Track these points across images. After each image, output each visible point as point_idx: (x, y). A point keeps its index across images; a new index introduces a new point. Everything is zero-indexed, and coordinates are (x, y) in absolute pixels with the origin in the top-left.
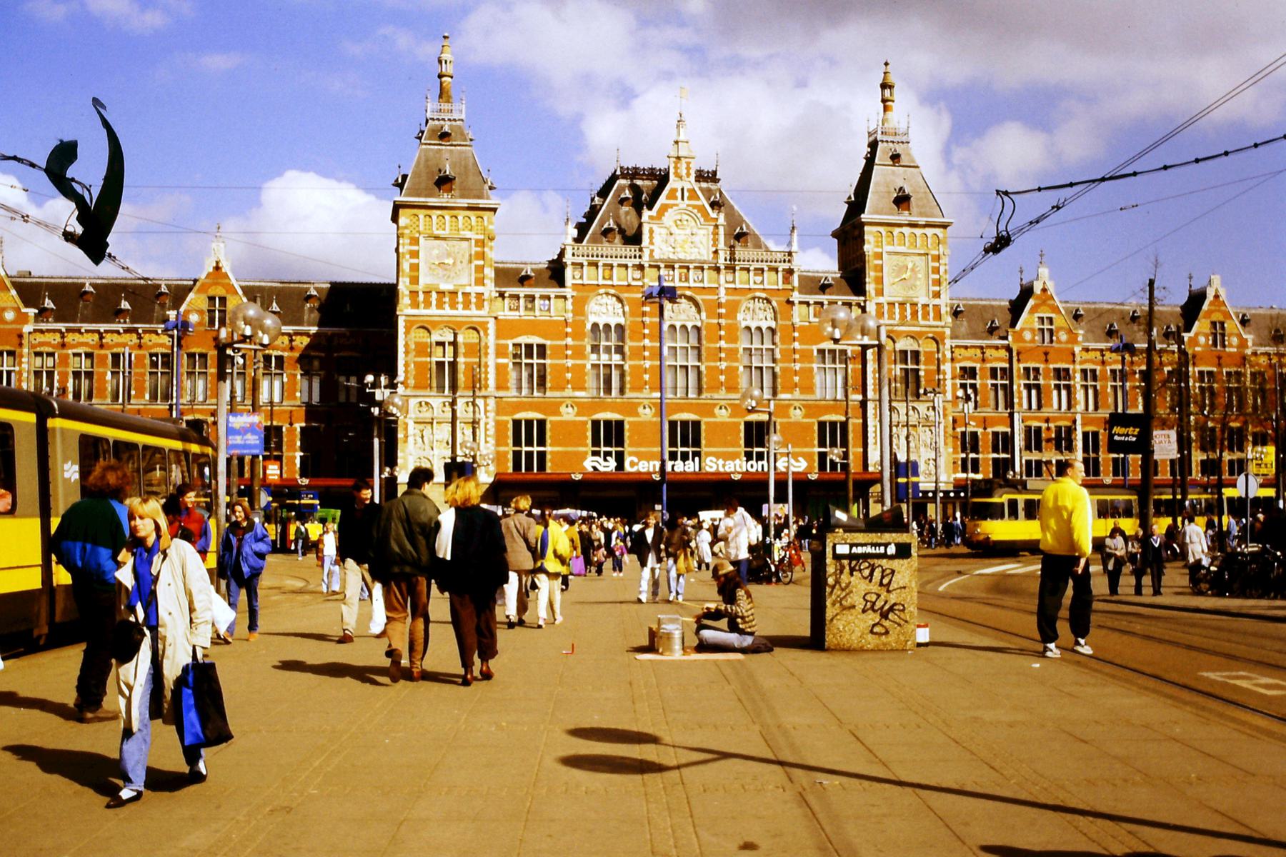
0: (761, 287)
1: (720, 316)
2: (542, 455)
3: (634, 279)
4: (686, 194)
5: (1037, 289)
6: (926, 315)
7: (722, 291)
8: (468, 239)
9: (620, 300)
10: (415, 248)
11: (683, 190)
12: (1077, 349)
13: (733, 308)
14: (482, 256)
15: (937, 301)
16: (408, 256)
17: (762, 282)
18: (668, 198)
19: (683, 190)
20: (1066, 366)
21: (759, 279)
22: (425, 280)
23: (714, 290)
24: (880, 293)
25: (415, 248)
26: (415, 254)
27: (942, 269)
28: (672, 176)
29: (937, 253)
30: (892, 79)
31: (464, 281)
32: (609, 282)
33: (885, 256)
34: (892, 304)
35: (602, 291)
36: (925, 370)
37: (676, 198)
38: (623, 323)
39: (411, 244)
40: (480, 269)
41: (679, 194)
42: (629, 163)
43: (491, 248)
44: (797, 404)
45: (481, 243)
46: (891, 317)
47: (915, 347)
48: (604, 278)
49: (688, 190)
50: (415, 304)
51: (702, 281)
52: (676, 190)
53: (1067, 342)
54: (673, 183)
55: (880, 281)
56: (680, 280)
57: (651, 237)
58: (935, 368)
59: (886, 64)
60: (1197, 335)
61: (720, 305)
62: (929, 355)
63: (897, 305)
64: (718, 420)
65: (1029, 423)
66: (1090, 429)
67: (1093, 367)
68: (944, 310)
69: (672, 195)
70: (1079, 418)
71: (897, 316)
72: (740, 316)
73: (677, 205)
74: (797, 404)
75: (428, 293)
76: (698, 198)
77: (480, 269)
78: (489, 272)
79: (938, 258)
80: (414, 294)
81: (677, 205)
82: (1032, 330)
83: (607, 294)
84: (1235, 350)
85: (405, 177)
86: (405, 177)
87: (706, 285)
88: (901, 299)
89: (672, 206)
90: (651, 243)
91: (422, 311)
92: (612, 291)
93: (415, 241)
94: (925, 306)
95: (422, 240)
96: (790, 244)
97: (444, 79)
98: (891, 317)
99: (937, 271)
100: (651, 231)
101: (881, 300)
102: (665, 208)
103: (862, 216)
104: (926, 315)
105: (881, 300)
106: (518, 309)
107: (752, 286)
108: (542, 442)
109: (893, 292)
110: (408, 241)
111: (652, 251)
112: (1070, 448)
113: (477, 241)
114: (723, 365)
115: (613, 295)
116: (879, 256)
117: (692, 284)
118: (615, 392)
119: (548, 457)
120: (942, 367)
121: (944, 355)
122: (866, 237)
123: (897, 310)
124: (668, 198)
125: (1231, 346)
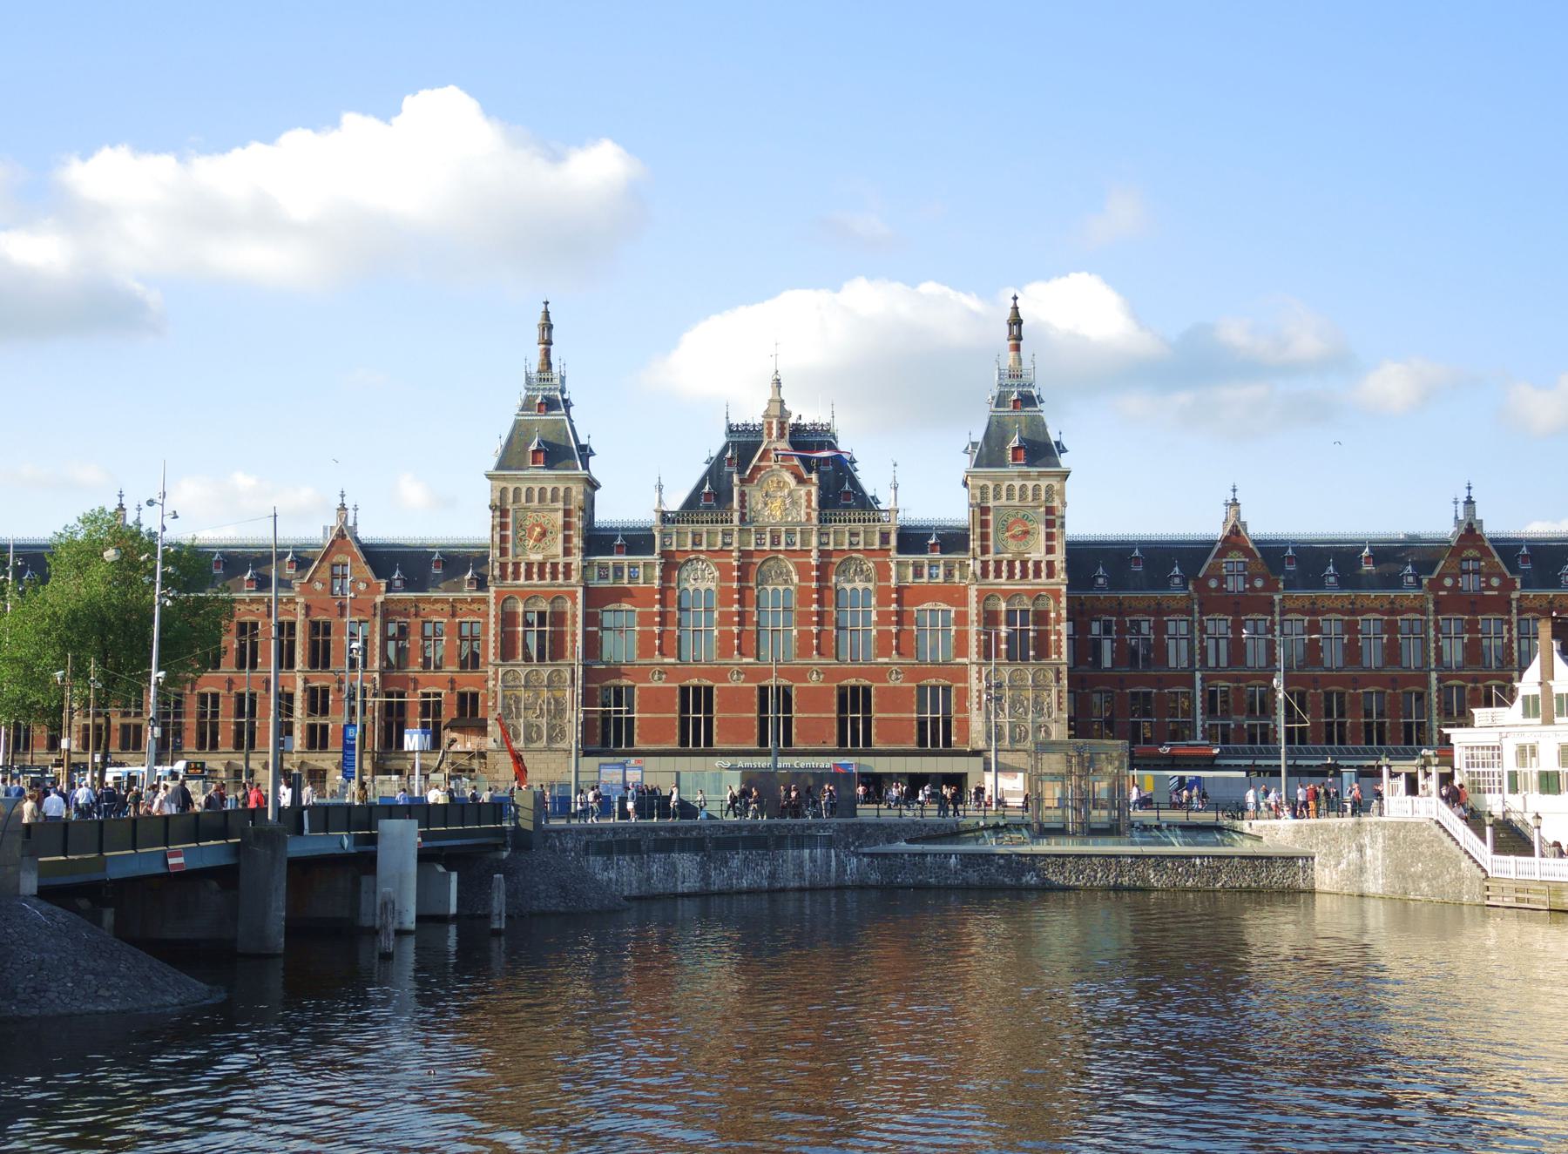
6: (1037, 574)
7: (814, 554)
12: (1277, 597)
35: (692, 556)
60: (1442, 576)
63: (1005, 562)
71: (1004, 575)
73: (771, 467)
84: (1496, 593)
94: (1037, 564)
98: (998, 575)
104: (1037, 574)
123: (1004, 568)
125: (1490, 587)
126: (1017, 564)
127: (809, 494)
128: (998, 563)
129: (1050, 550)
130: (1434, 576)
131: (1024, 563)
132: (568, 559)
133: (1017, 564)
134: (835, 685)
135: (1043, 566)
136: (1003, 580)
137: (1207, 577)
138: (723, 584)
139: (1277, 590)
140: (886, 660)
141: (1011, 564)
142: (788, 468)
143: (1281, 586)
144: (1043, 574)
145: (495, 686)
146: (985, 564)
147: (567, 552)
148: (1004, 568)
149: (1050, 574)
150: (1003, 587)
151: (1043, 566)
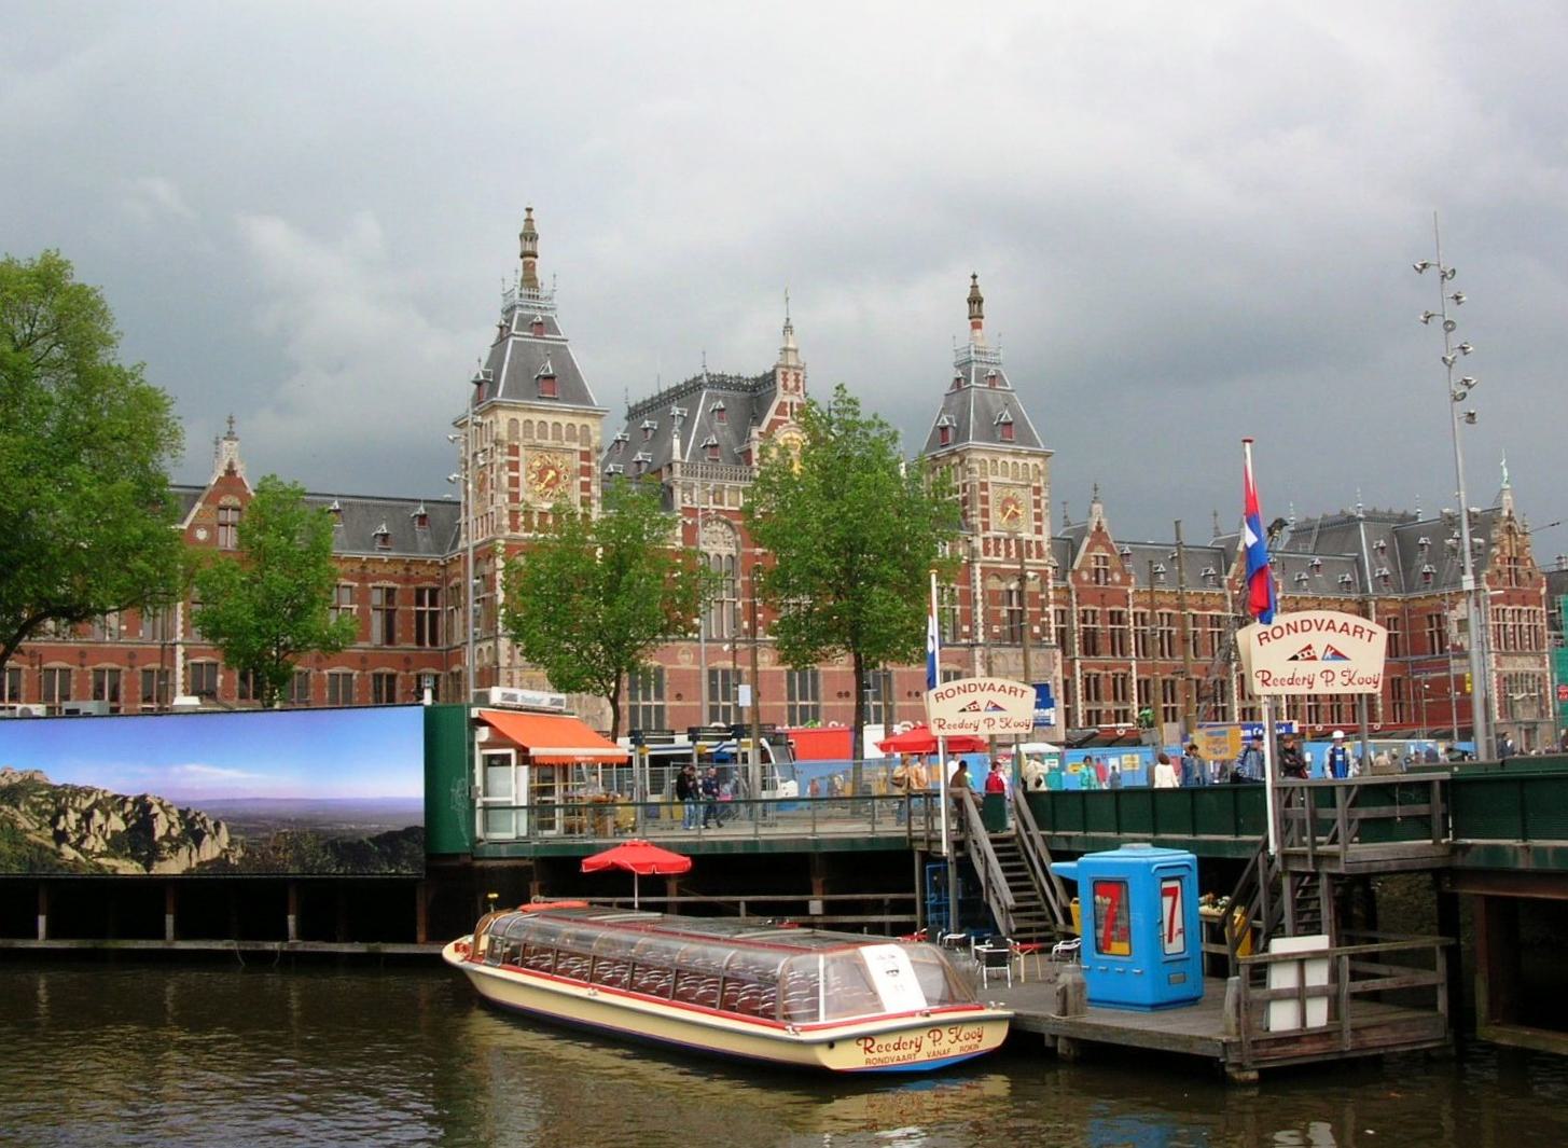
2: (659, 709)
8: (572, 451)
9: (730, 525)
10: (514, 459)
11: (792, 404)
12: (1130, 591)
15: (1039, 537)
16: (507, 468)
19: (792, 404)
20: (1120, 609)
24: (986, 527)
25: (514, 459)
26: (514, 466)
27: (1043, 503)
28: (780, 390)
30: (983, 292)
33: (990, 486)
34: (997, 540)
38: (734, 554)
39: (510, 454)
41: (788, 409)
42: (716, 370)
49: (799, 405)
52: (785, 404)
54: (782, 396)
55: (985, 513)
59: (974, 277)
65: (1089, 670)
66: (1144, 676)
67: (1143, 610)
68: (1046, 547)
70: (1134, 663)
71: (1003, 553)
73: (786, 422)
77: (585, 487)
80: (514, 514)
82: (1089, 570)
83: (718, 520)
88: (1006, 534)
89: (781, 422)
91: (523, 534)
92: (724, 517)
93: (514, 450)
95: (522, 451)
101: (988, 534)
105: (988, 534)
108: (659, 696)
110: (506, 450)
112: (1126, 697)
113: (582, 452)
115: (725, 522)
116: (984, 486)
118: (1437, 654)
119: (667, 712)
123: (1002, 546)
124: (777, 412)
126: (1013, 543)
129: (1039, 530)
130: (1230, 577)
133: (1013, 543)
135: (1033, 546)
138: (744, 550)
141: (1007, 541)
144: (1034, 554)
146: (986, 540)
147: (585, 502)
148: (1002, 546)
150: (1003, 566)
151: (1033, 546)
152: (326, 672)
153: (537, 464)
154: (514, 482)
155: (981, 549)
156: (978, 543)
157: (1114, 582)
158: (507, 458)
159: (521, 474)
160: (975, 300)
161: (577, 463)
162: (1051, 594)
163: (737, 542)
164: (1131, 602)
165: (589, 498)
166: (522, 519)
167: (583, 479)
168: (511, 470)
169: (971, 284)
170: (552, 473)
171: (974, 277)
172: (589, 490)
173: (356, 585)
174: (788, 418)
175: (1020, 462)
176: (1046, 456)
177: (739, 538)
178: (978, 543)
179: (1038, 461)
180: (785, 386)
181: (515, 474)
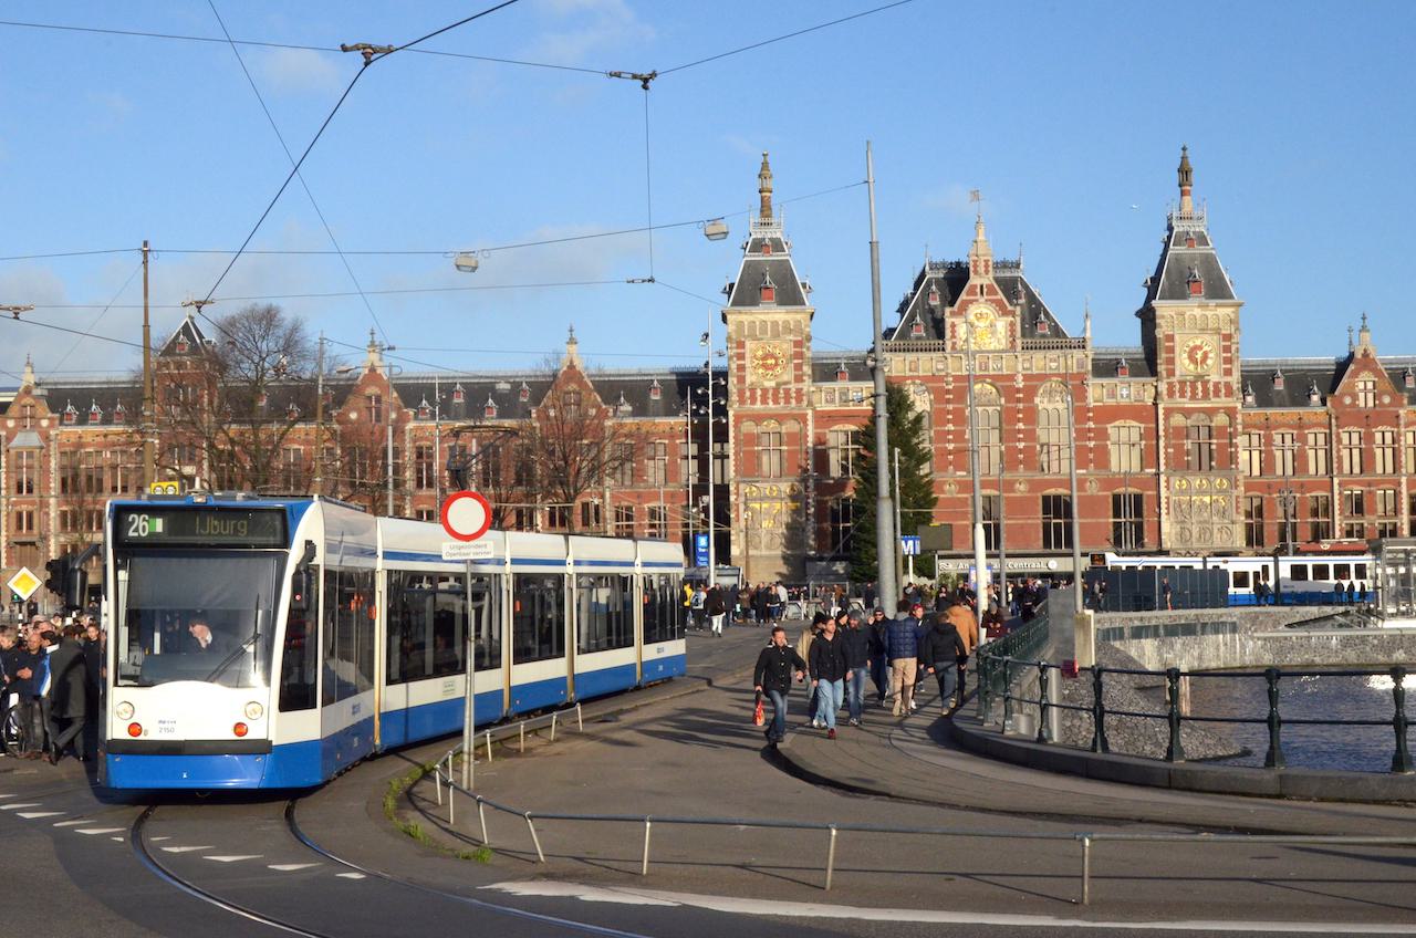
0: (1056, 372)
1: (1019, 400)
3: (938, 370)
4: (985, 290)
5: (1359, 355)
6: (1217, 394)
7: (1020, 378)
10: (742, 351)
11: (982, 287)
12: (1402, 412)
13: (1030, 392)
14: (799, 355)
15: (1228, 379)
17: (1058, 368)
18: (968, 295)
19: (982, 287)
21: (1054, 365)
22: (749, 380)
23: (1011, 378)
24: (1171, 373)
25: (742, 351)
26: (741, 357)
27: (1233, 348)
28: (972, 274)
29: (1228, 332)
30: (1192, 163)
31: (785, 378)
32: (915, 374)
36: (1216, 444)
37: (976, 295)
39: (737, 348)
40: (798, 367)
41: (978, 290)
43: (808, 349)
44: (1092, 478)
45: (798, 344)
46: (1182, 395)
47: (1207, 423)
48: (910, 370)
50: (742, 401)
51: (1001, 369)
52: (976, 286)
53: (1390, 405)
54: (974, 280)
55: (1171, 361)
56: (981, 369)
57: (953, 332)
58: (1228, 441)
59: (1184, 149)
61: (1018, 391)
62: (1221, 429)
64: (1018, 495)
69: (972, 292)
70: (1404, 480)
72: (1037, 400)
73: (977, 300)
74: (1092, 478)
75: (753, 391)
76: (996, 294)
78: (807, 369)
79: (1228, 337)
80: (741, 393)
81: (977, 300)
83: (914, 383)
85: (732, 286)
86: (732, 286)
87: (1005, 372)
89: (971, 302)
90: (953, 336)
92: (918, 382)
93: (741, 345)
94: (1216, 385)
96: (1085, 330)
97: (764, 194)
99: (1227, 349)
100: (953, 326)
102: (966, 304)
103: (1153, 302)
104: (1217, 394)
106: (833, 401)
107: (1048, 372)
109: (1184, 366)
110: (734, 345)
111: (954, 344)
114: (1021, 445)
117: (991, 373)
120: (1234, 441)
121: (1236, 429)
122: (1158, 321)
123: (1189, 389)
126: (1199, 385)
127: (1012, 324)
128: (1183, 383)
129: (1228, 372)
131: (1205, 384)
132: (800, 386)
133: (1199, 385)
134: (1039, 495)
136: (1185, 400)
137: (1343, 395)
139: (1402, 406)
140: (1084, 471)
142: (993, 301)
143: (1405, 401)
145: (736, 499)
146: (1171, 386)
147: (799, 379)
149: (1229, 393)
150: (1186, 406)
152: (646, 506)
153: (760, 353)
154: (741, 368)
155: (1165, 392)
156: (1163, 387)
157: (1382, 405)
158: (735, 351)
159: (747, 362)
160: (1184, 172)
161: (788, 348)
162: (1240, 428)
163: (931, 401)
164: (1402, 422)
165: (802, 376)
166: (748, 394)
167: (796, 361)
168: (738, 359)
169: (1181, 155)
170: (773, 361)
171: (1184, 149)
172: (801, 369)
173: (667, 442)
174: (979, 296)
175: (1209, 314)
176: (1240, 305)
177: (932, 397)
178: (1163, 387)
179: (1229, 310)
180: (976, 272)
181: (742, 362)
